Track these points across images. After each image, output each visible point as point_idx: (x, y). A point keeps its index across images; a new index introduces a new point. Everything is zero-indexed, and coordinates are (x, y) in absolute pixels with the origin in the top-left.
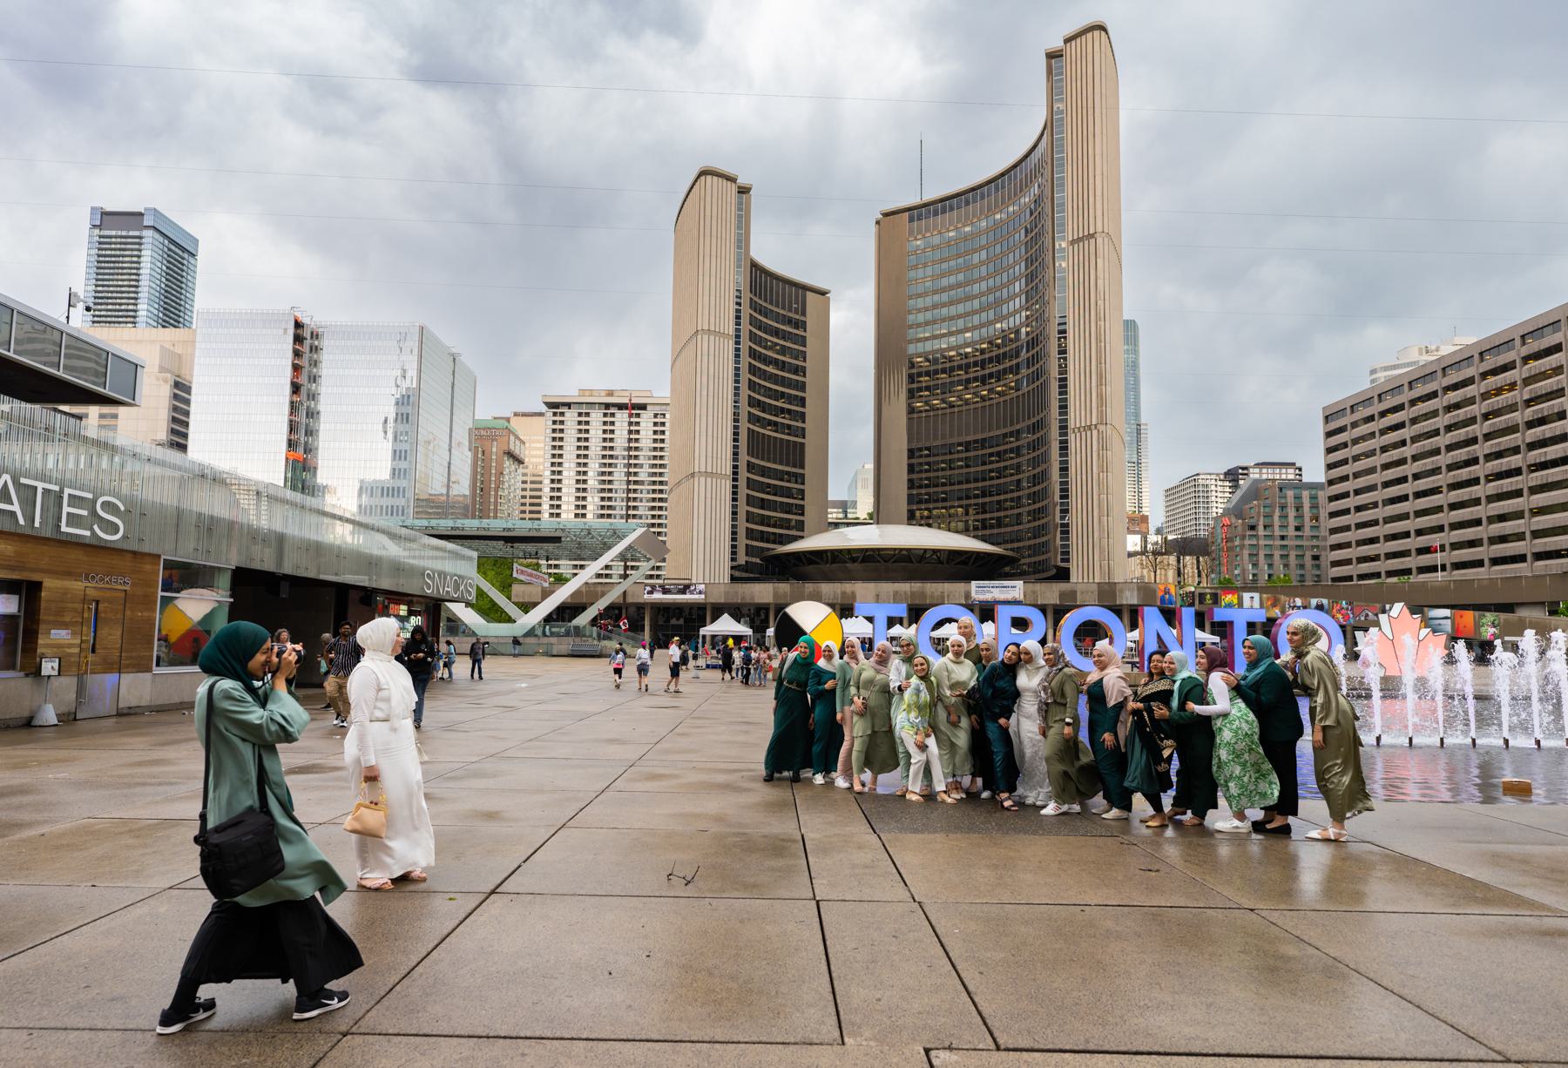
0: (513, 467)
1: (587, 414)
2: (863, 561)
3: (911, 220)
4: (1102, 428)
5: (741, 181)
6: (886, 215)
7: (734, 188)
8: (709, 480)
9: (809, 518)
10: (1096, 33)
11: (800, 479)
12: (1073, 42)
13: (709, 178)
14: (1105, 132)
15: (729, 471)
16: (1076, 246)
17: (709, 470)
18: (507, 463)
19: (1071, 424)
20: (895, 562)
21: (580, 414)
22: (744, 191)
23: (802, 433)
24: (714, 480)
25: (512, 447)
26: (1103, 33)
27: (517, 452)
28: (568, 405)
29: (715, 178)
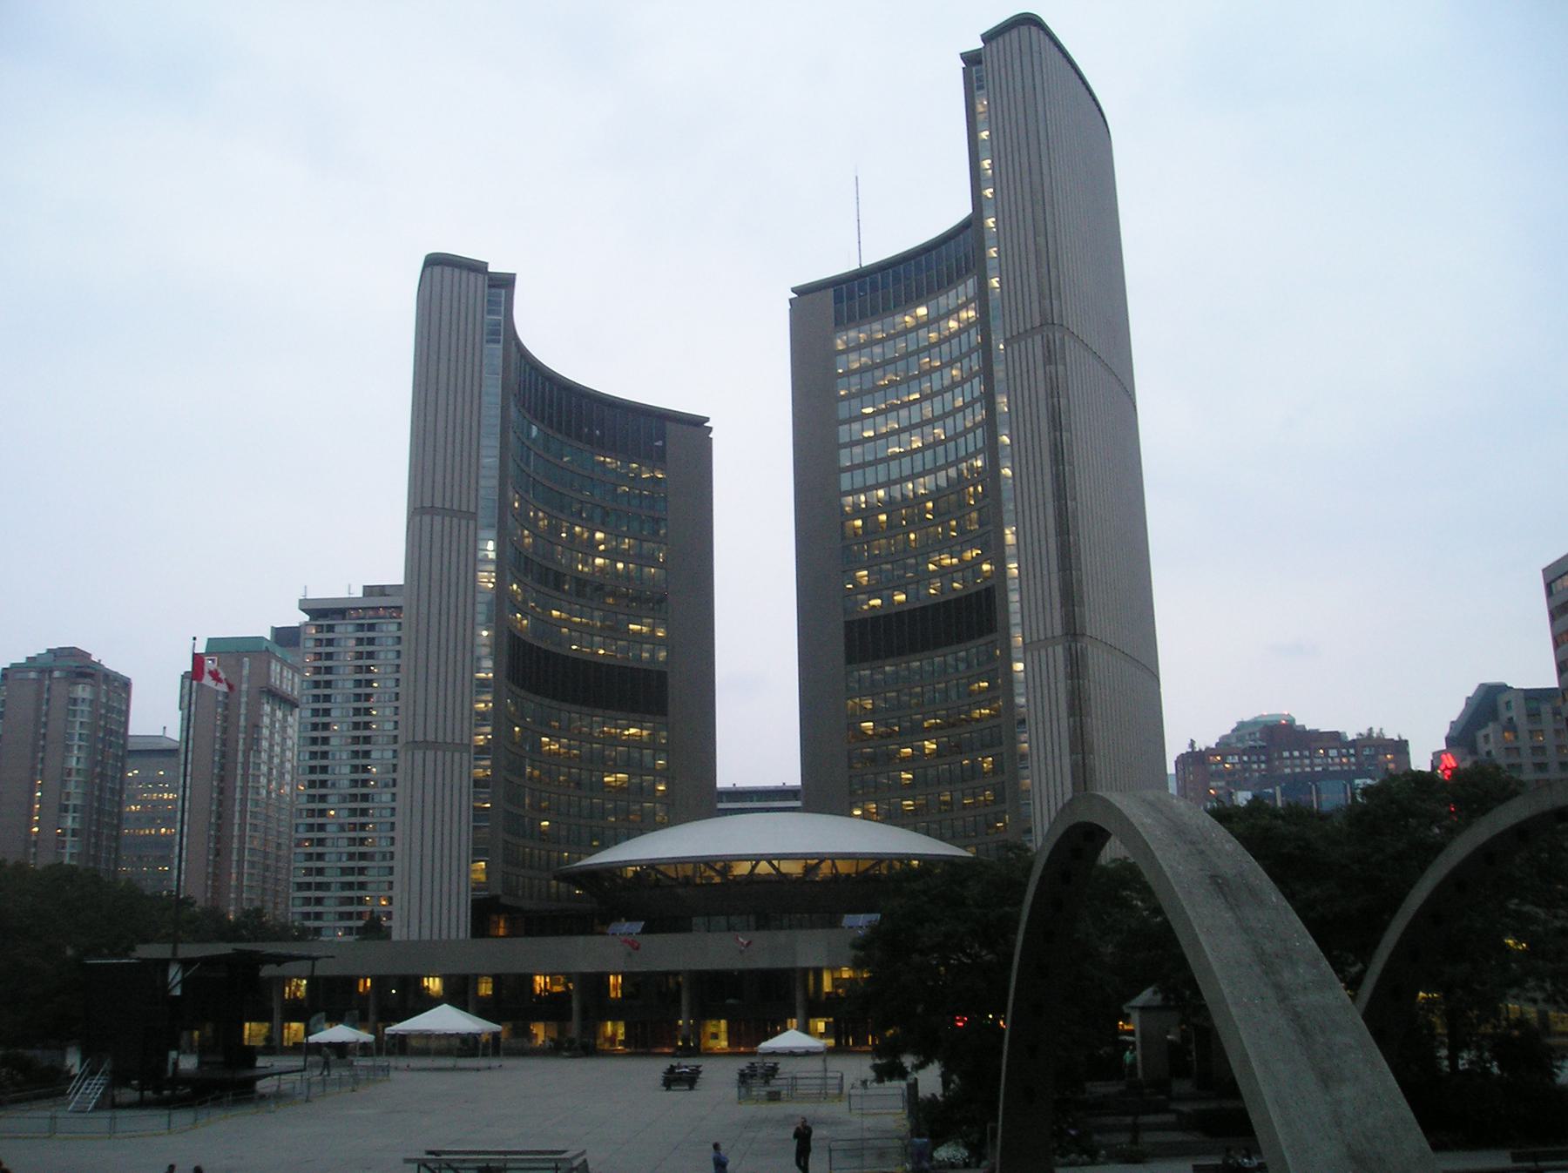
0: (279, 714)
3: (838, 299)
6: (802, 291)
8: (430, 754)
10: (1024, 29)
12: (994, 44)
13: (437, 269)
14: (1045, 171)
16: (1016, 346)
17: (431, 737)
18: (267, 708)
22: (505, 283)
24: (440, 753)
25: (275, 681)
26: (1034, 29)
27: (286, 687)
29: (448, 270)
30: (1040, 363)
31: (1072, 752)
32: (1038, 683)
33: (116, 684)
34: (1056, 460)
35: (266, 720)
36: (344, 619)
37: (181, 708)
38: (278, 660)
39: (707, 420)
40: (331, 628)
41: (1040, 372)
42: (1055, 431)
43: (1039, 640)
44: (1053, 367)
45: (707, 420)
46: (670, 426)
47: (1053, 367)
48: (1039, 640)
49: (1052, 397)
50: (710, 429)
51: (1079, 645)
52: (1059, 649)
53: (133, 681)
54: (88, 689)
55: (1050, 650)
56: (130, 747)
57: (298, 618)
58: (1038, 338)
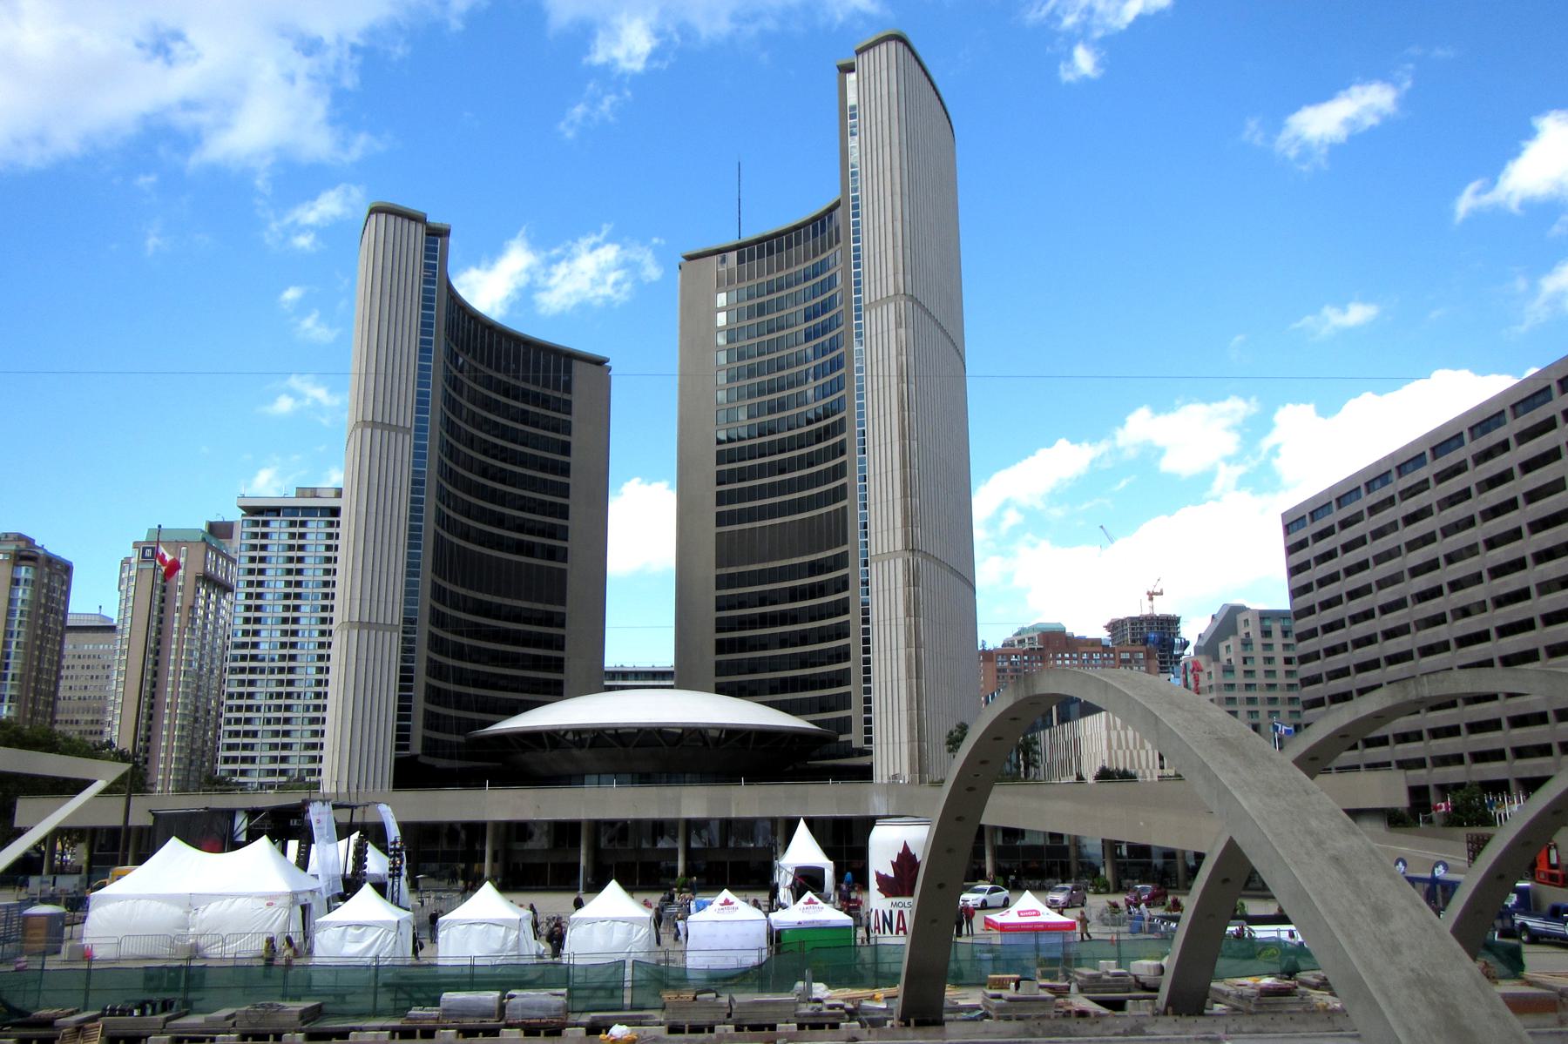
1: (303, 524)
2: (592, 746)
4: (908, 555)
5: (433, 219)
6: (690, 258)
9: (569, 676)
10: (892, 44)
11: (558, 620)
12: (866, 56)
13: (382, 217)
15: (398, 619)
19: (872, 551)
20: (637, 746)
21: (293, 524)
23: (562, 554)
25: (211, 568)
26: (901, 45)
27: (221, 574)
28: (276, 511)
29: (392, 218)
30: (892, 326)
31: (908, 646)
32: (881, 588)
33: (58, 567)
35: (201, 602)
36: (279, 515)
37: (119, 590)
38: (214, 549)
39: (608, 360)
40: (266, 524)
41: (893, 334)
43: (883, 553)
45: (608, 360)
46: (577, 365)
47: (902, 331)
48: (883, 553)
50: (610, 369)
52: (900, 562)
53: (74, 565)
54: (31, 570)
55: (892, 562)
56: (69, 624)
57: (235, 515)
58: (892, 306)
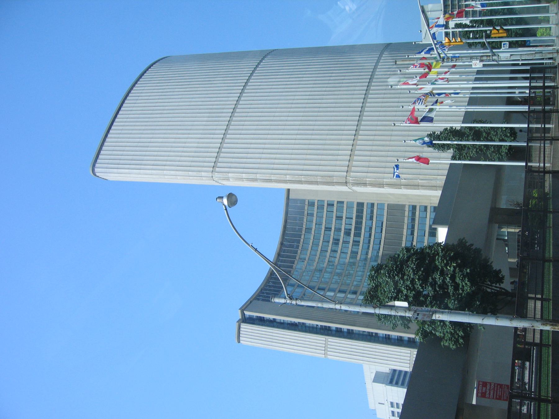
7: (243, 326)
26: (96, 170)
34: (270, 182)
42: (257, 181)
44: (230, 179)
49: (243, 180)
51: (351, 181)
